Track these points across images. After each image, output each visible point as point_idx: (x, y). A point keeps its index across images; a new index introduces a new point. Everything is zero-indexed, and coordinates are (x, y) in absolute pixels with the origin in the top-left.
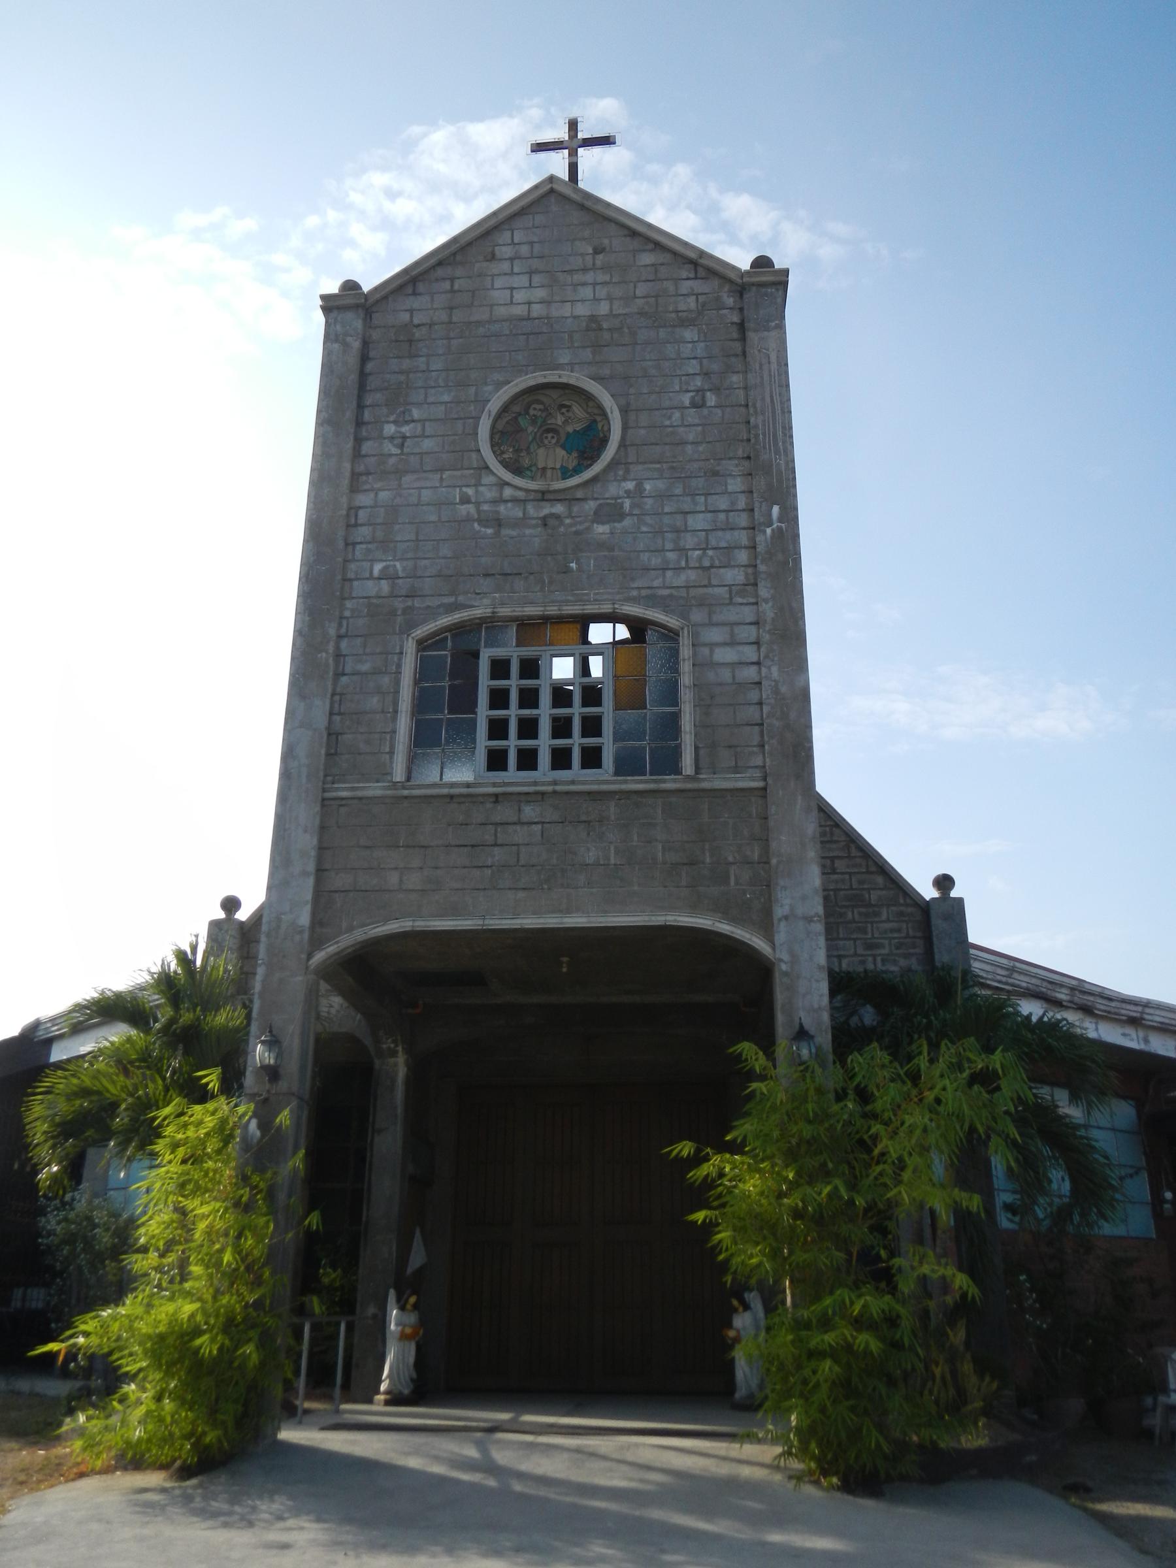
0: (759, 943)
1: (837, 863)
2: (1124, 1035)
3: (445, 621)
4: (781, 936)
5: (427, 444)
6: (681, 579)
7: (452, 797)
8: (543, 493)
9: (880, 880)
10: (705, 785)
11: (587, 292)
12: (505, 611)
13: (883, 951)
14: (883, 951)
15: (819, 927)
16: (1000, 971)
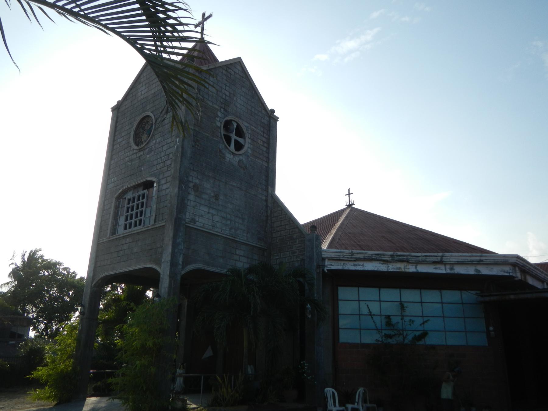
0: (159, 269)
1: (287, 226)
2: (435, 268)
3: (120, 191)
4: (162, 268)
5: (124, 142)
6: (159, 167)
7: (116, 239)
8: (140, 149)
9: (297, 230)
10: (158, 226)
11: (154, 86)
12: (129, 186)
13: (297, 254)
14: (297, 254)
15: (169, 264)
16: (345, 254)
